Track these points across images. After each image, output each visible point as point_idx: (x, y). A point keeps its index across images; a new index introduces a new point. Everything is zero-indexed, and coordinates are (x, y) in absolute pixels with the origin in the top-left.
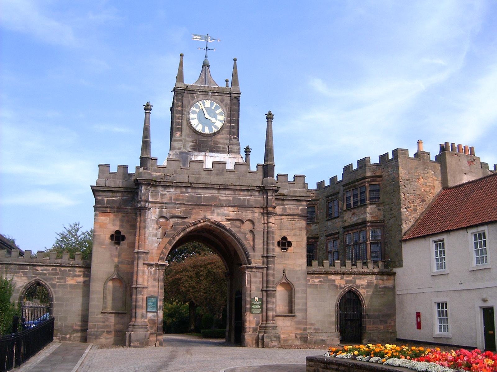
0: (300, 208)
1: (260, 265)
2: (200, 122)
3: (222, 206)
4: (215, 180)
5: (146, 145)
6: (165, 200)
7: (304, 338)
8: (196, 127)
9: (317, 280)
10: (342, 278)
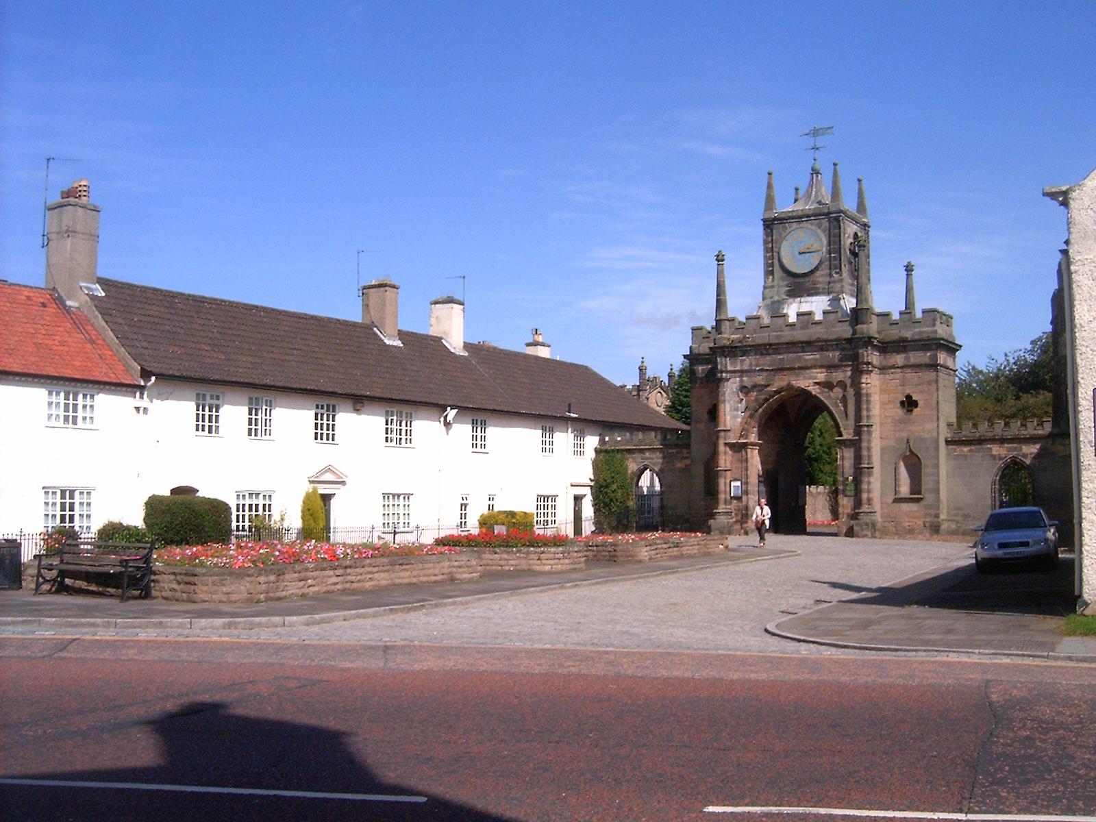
0: (928, 354)
4: (800, 335)
5: (720, 304)
6: (745, 367)
7: (935, 527)
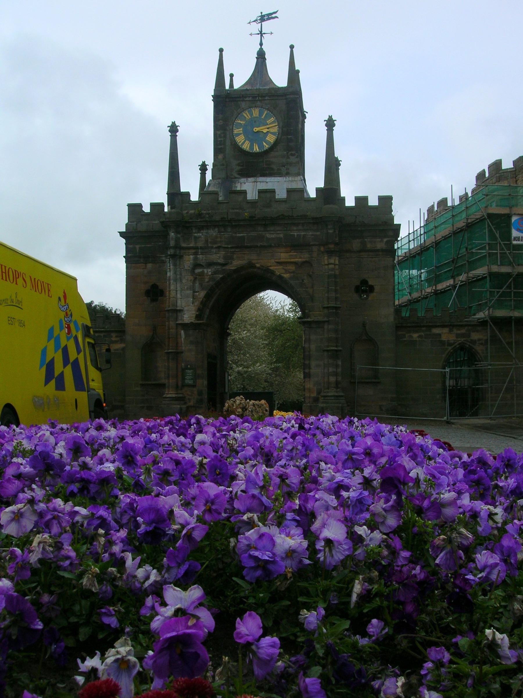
0: (385, 240)
1: (320, 319)
2: (247, 138)
3: (270, 246)
6: (200, 244)
9: (415, 336)
10: (451, 331)
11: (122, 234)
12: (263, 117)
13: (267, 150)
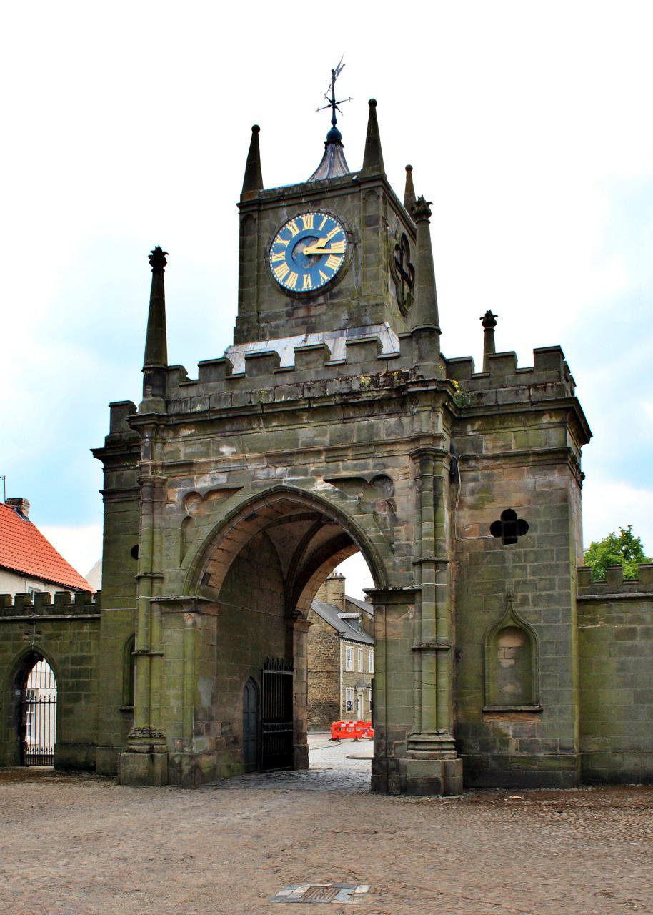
8: (285, 279)
11: (97, 453)
12: (320, 229)
13: (326, 285)
